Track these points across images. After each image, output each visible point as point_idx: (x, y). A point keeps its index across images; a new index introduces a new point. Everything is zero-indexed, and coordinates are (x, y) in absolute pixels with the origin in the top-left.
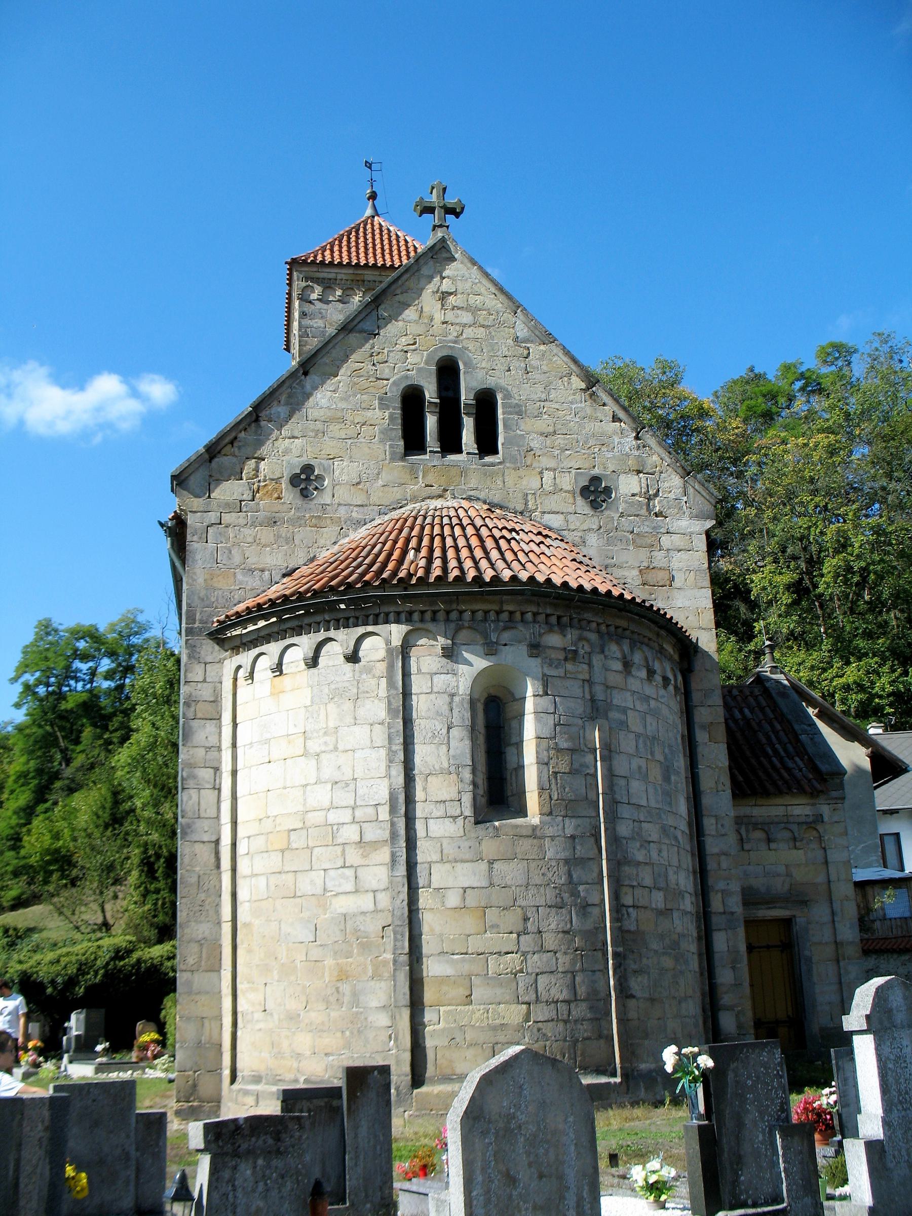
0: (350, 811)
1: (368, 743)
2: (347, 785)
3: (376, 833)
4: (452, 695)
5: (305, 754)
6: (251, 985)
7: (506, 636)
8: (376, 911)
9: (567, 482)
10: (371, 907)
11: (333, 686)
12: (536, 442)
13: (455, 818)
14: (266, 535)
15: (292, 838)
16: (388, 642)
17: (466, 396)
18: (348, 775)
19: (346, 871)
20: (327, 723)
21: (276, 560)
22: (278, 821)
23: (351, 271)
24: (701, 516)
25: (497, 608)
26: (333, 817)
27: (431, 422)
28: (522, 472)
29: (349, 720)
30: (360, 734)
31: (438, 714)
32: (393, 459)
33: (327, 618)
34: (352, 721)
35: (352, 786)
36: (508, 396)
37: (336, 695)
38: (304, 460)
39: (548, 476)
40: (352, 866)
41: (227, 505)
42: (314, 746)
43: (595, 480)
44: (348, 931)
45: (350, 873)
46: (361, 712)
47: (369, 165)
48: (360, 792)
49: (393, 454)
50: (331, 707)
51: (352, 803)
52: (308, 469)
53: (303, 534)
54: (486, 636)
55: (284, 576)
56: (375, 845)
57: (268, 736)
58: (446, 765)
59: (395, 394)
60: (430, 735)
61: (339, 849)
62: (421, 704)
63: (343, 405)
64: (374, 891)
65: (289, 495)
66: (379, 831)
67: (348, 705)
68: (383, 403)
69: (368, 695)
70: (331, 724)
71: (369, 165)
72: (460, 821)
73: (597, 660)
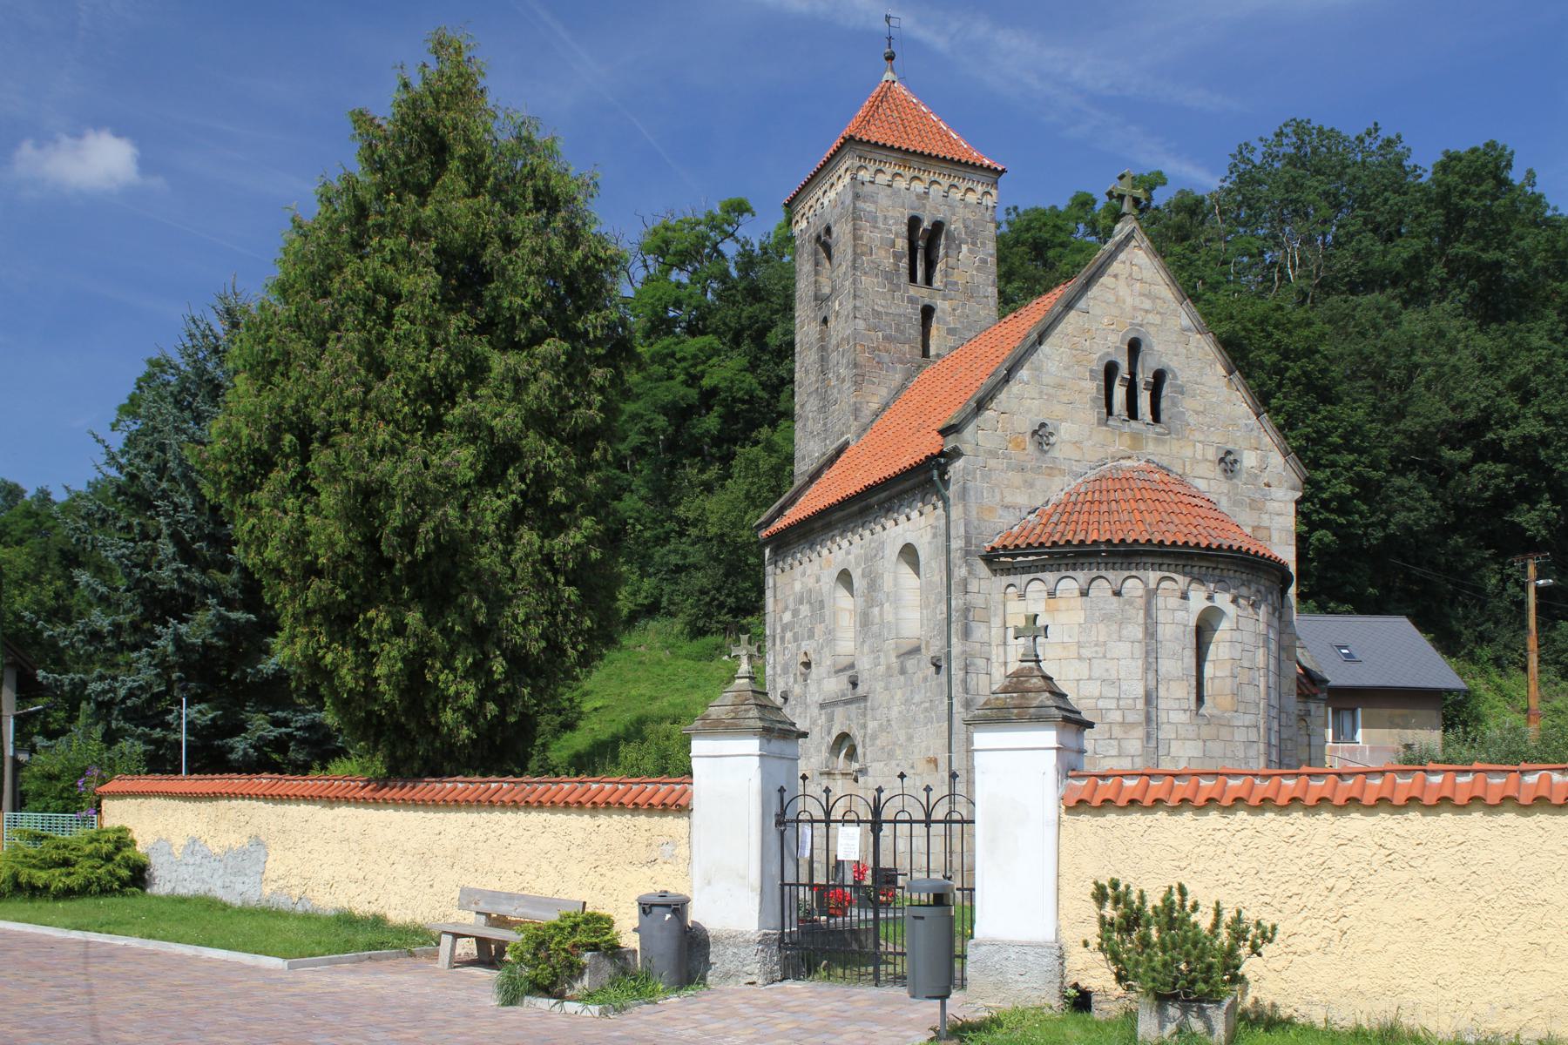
4: (1185, 626)
5: (1080, 658)
12: (1192, 419)
14: (1017, 478)
16: (1146, 585)
17: (1144, 376)
18: (1114, 676)
21: (1022, 499)
23: (900, 155)
24: (1294, 488)
26: (1101, 704)
27: (1120, 393)
28: (1182, 443)
29: (1115, 637)
30: (1122, 649)
31: (1177, 639)
32: (1099, 424)
36: (1175, 377)
37: (1107, 618)
38: (1041, 419)
41: (990, 451)
42: (1086, 653)
43: (1229, 453)
45: (1114, 743)
46: (1124, 632)
48: (1123, 688)
49: (1099, 419)
50: (1101, 626)
52: (1043, 425)
53: (1040, 481)
56: (1133, 725)
59: (1100, 368)
61: (1107, 727)
62: (1166, 631)
65: (1031, 447)
67: (1115, 627)
70: (1101, 639)
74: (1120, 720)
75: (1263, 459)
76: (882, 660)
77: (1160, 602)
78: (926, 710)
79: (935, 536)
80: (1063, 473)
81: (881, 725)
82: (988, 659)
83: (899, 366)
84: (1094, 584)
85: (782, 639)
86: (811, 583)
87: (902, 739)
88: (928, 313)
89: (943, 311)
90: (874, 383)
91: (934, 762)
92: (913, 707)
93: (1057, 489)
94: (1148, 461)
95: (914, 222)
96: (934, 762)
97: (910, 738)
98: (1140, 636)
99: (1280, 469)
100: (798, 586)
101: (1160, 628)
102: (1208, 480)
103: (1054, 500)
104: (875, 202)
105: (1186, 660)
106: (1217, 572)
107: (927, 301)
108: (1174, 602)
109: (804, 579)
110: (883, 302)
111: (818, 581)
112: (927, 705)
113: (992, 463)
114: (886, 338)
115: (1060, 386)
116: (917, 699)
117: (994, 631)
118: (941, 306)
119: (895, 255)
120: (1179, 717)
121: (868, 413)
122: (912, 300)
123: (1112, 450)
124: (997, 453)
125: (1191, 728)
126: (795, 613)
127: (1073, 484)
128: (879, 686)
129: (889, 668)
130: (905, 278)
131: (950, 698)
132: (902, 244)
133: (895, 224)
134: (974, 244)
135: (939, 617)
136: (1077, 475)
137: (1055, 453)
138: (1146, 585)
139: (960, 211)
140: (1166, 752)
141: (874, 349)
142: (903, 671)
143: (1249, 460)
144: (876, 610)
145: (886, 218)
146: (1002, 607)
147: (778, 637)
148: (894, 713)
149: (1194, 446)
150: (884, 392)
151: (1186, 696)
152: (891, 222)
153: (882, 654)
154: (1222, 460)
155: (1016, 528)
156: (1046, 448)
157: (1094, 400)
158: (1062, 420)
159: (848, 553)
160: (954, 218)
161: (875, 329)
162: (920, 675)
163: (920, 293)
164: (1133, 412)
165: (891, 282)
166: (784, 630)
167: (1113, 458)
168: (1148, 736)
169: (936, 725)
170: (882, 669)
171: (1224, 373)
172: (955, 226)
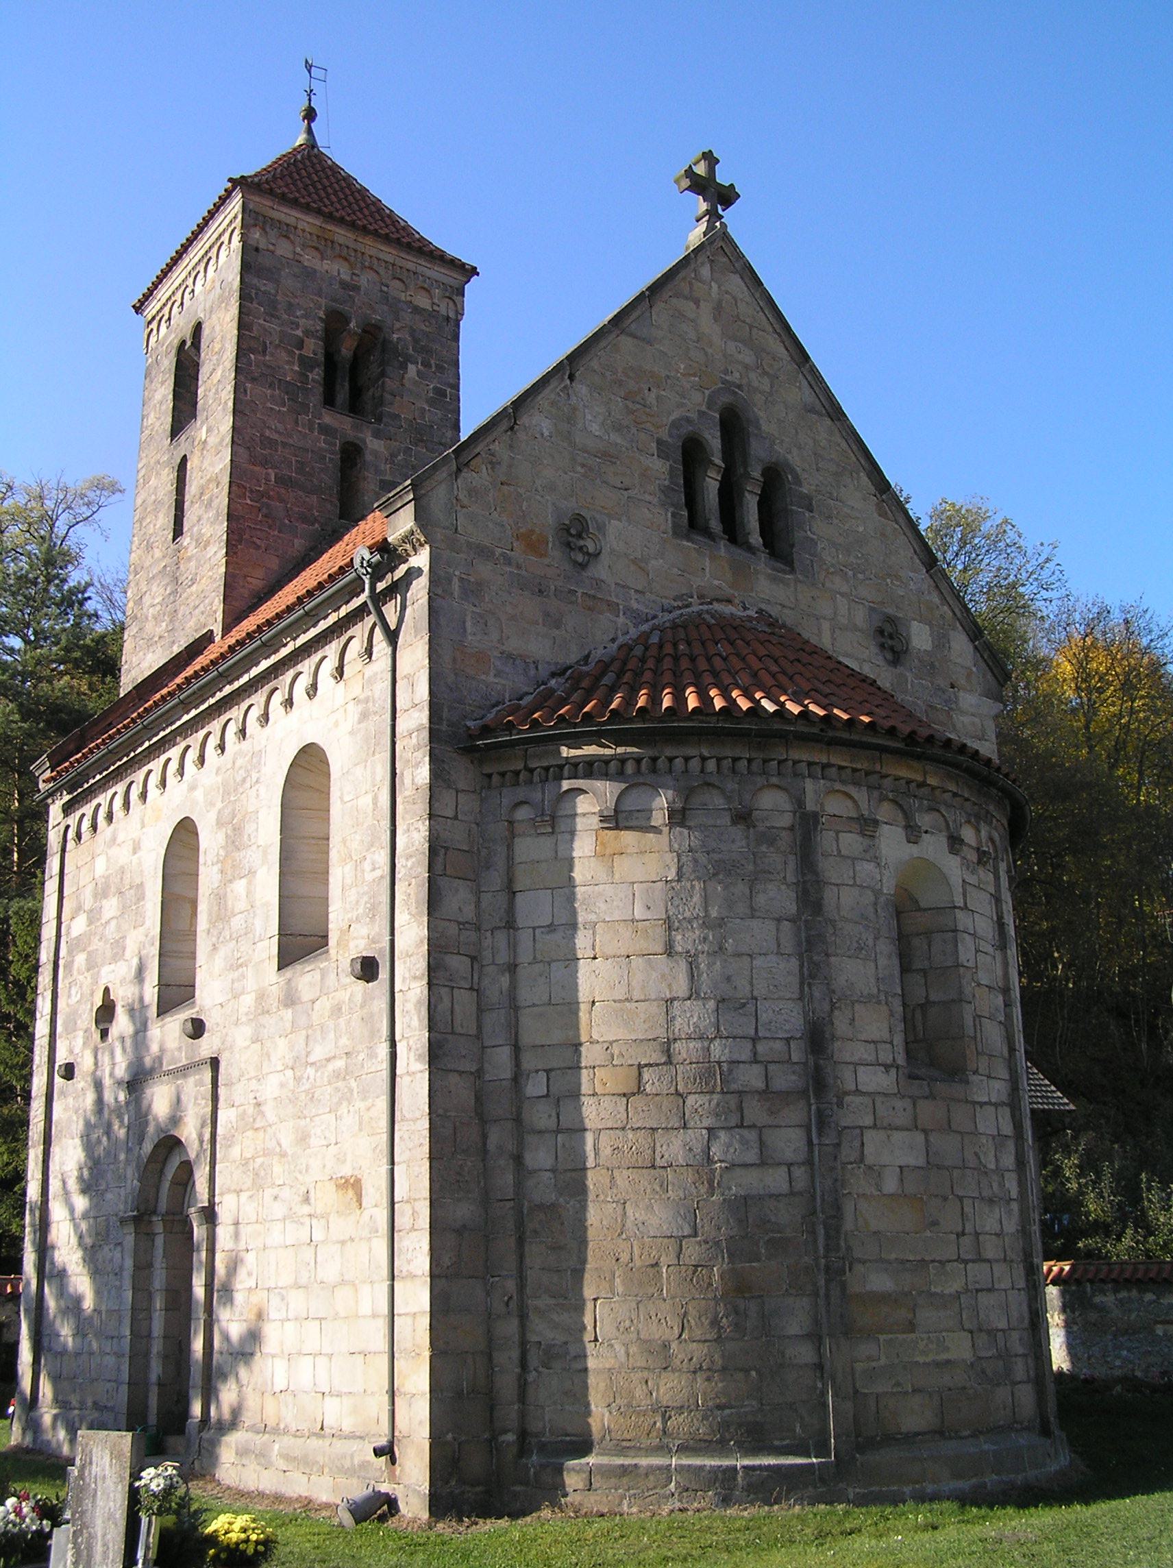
0: (749, 1045)
1: (774, 947)
2: (744, 1005)
3: (785, 1080)
6: (561, 1301)
8: (792, 1193)
10: (784, 1187)
11: (716, 856)
13: (887, 1067)
15: (646, 1076)
16: (800, 803)
18: (743, 989)
19: (745, 1132)
20: (706, 911)
22: (616, 1050)
25: (919, 778)
29: (742, 909)
30: (761, 933)
32: (677, 534)
33: (706, 754)
34: (748, 911)
35: (750, 1008)
36: (798, 481)
40: (753, 1126)
44: (750, 1220)
45: (752, 1135)
46: (761, 900)
48: (764, 1017)
51: (752, 1032)
54: (907, 816)
55: (553, 675)
56: (785, 1097)
57: (593, 917)
58: (875, 991)
60: (855, 945)
61: (733, 1101)
63: (615, 438)
64: (790, 1165)
65: (555, 553)
66: (794, 1078)
67: (741, 888)
68: (663, 450)
69: (771, 877)
70: (714, 913)
71: (309, 67)
72: (893, 1071)
74: (760, 1085)
75: (941, 641)
76: (251, 984)
77: (826, 840)
78: (337, 1075)
79: (364, 716)
80: (613, 607)
81: (242, 1116)
82: (473, 959)
83: (301, 527)
84: (696, 801)
85: (69, 966)
86: (122, 855)
87: (287, 1139)
88: (351, 455)
89: (376, 454)
90: (258, 547)
91: (353, 1186)
92: (310, 1071)
94: (760, 611)
95: (335, 323)
96: (353, 1186)
97: (303, 1139)
98: (792, 908)
99: (969, 662)
100: (100, 867)
101: (829, 895)
103: (598, 654)
104: (277, 282)
105: (882, 962)
106: (924, 791)
107: (351, 434)
108: (851, 841)
109: (114, 851)
110: (280, 427)
111: (136, 849)
112: (340, 1064)
113: (484, 570)
114: (280, 480)
115: (608, 456)
116: (318, 1053)
117: (486, 898)
118: (374, 445)
119: (303, 360)
120: (875, 1080)
121: (246, 593)
122: (325, 429)
123: (697, 582)
124: (493, 553)
125: (899, 1104)
126: (94, 916)
127: (634, 633)
128: (241, 1036)
129: (261, 996)
130: (315, 399)
131: (393, 1044)
132: (313, 347)
133: (305, 316)
134: (426, 365)
135: (369, 876)
136: (638, 618)
137: (600, 570)
138: (800, 803)
139: (407, 317)
140: (854, 1156)
141: (263, 495)
142: (290, 1000)
143: (920, 638)
144: (240, 886)
145: (290, 305)
146: (501, 850)
147: (61, 962)
148: (270, 1088)
149: (833, 599)
150: (274, 563)
151: (886, 1035)
152: (298, 313)
153: (250, 972)
154: (881, 632)
155: (530, 698)
156: (580, 558)
157: (665, 491)
158: (610, 516)
159: (192, 788)
160: (397, 325)
161: (264, 463)
162: (324, 1005)
163: (342, 423)
165: (293, 400)
166: (70, 952)
167: (700, 597)
168: (823, 1121)
169: (360, 1105)
170: (248, 1000)
171: (872, 489)
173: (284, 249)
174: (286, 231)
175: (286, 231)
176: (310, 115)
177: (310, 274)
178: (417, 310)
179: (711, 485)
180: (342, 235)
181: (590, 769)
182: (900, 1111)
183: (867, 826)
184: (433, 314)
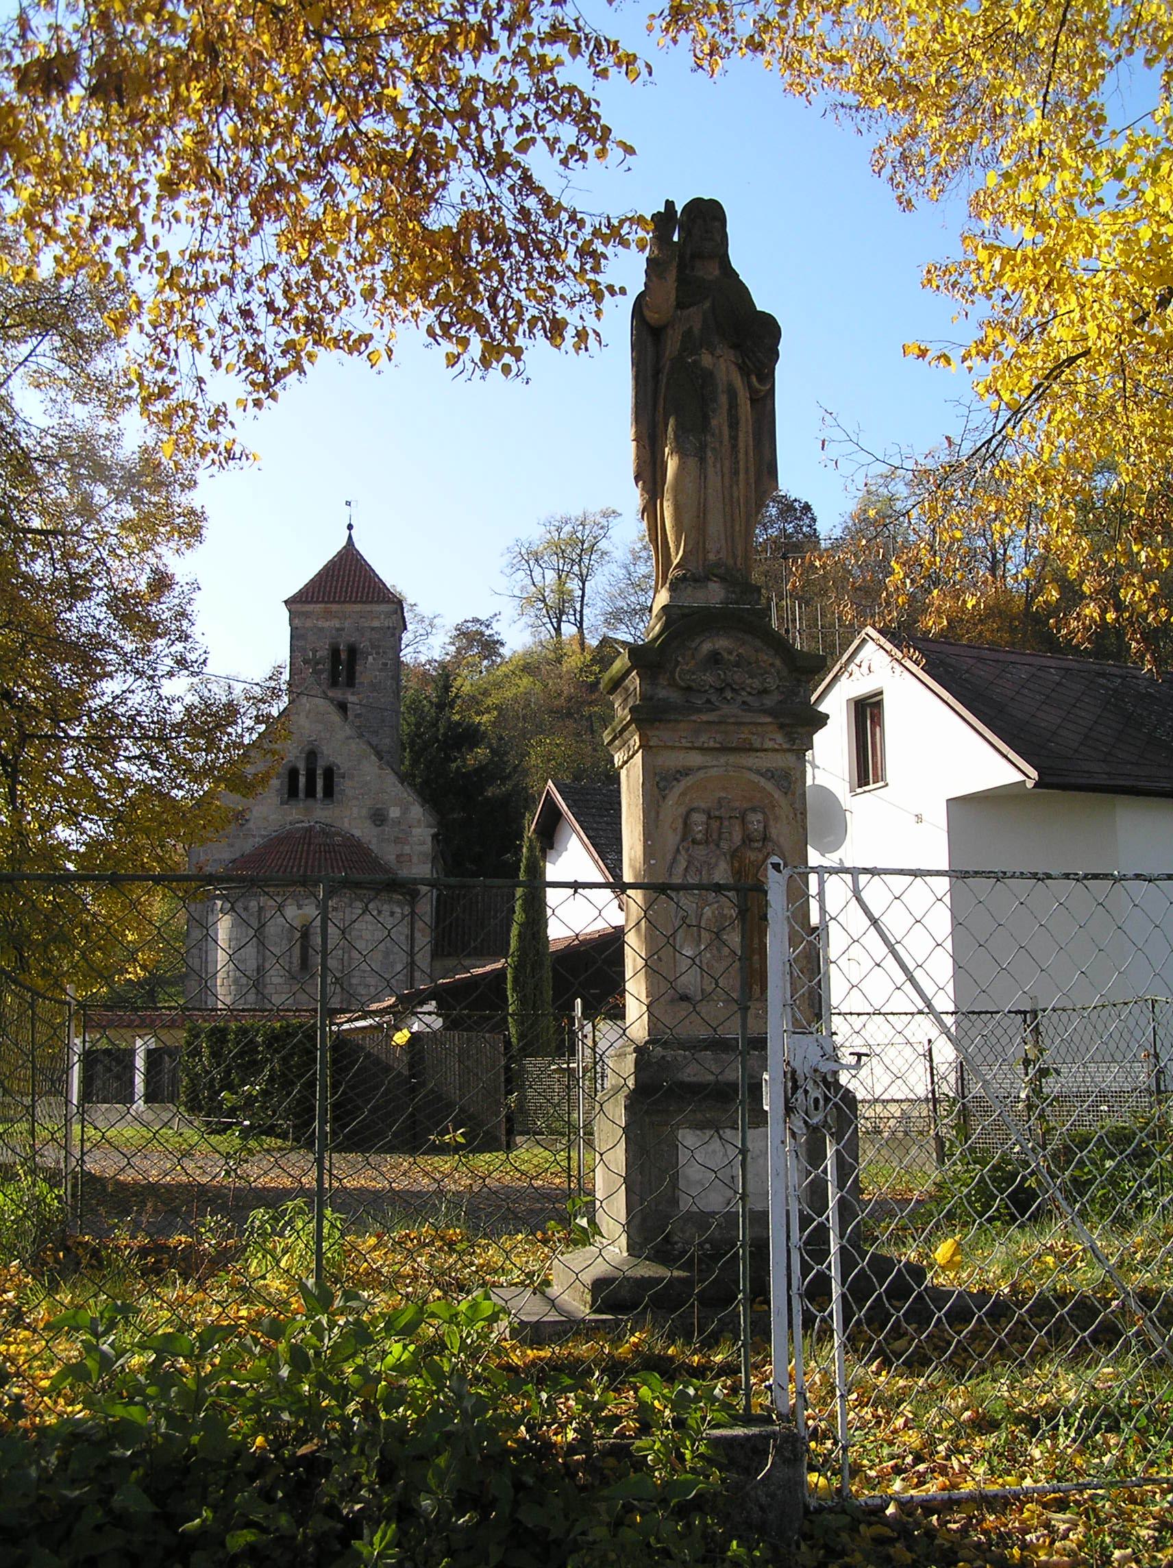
7: (306, 902)
9: (364, 812)
12: (350, 793)
32: (282, 803)
36: (339, 768)
39: (355, 810)
47: (348, 503)
71: (348, 503)
73: (348, 910)
75: (405, 811)
80: (254, 836)
93: (248, 846)
102: (362, 830)
134: (378, 653)
136: (263, 837)
137: (251, 825)
143: (394, 812)
163: (337, 694)
164: (311, 792)
172: (363, 645)
173: (309, 624)
174: (307, 615)
175: (307, 615)
176: (350, 527)
177: (321, 629)
178: (373, 629)
179: (302, 780)
180: (334, 607)
181: (218, 897)
182: (286, 988)
183: (280, 908)
184: (381, 628)
